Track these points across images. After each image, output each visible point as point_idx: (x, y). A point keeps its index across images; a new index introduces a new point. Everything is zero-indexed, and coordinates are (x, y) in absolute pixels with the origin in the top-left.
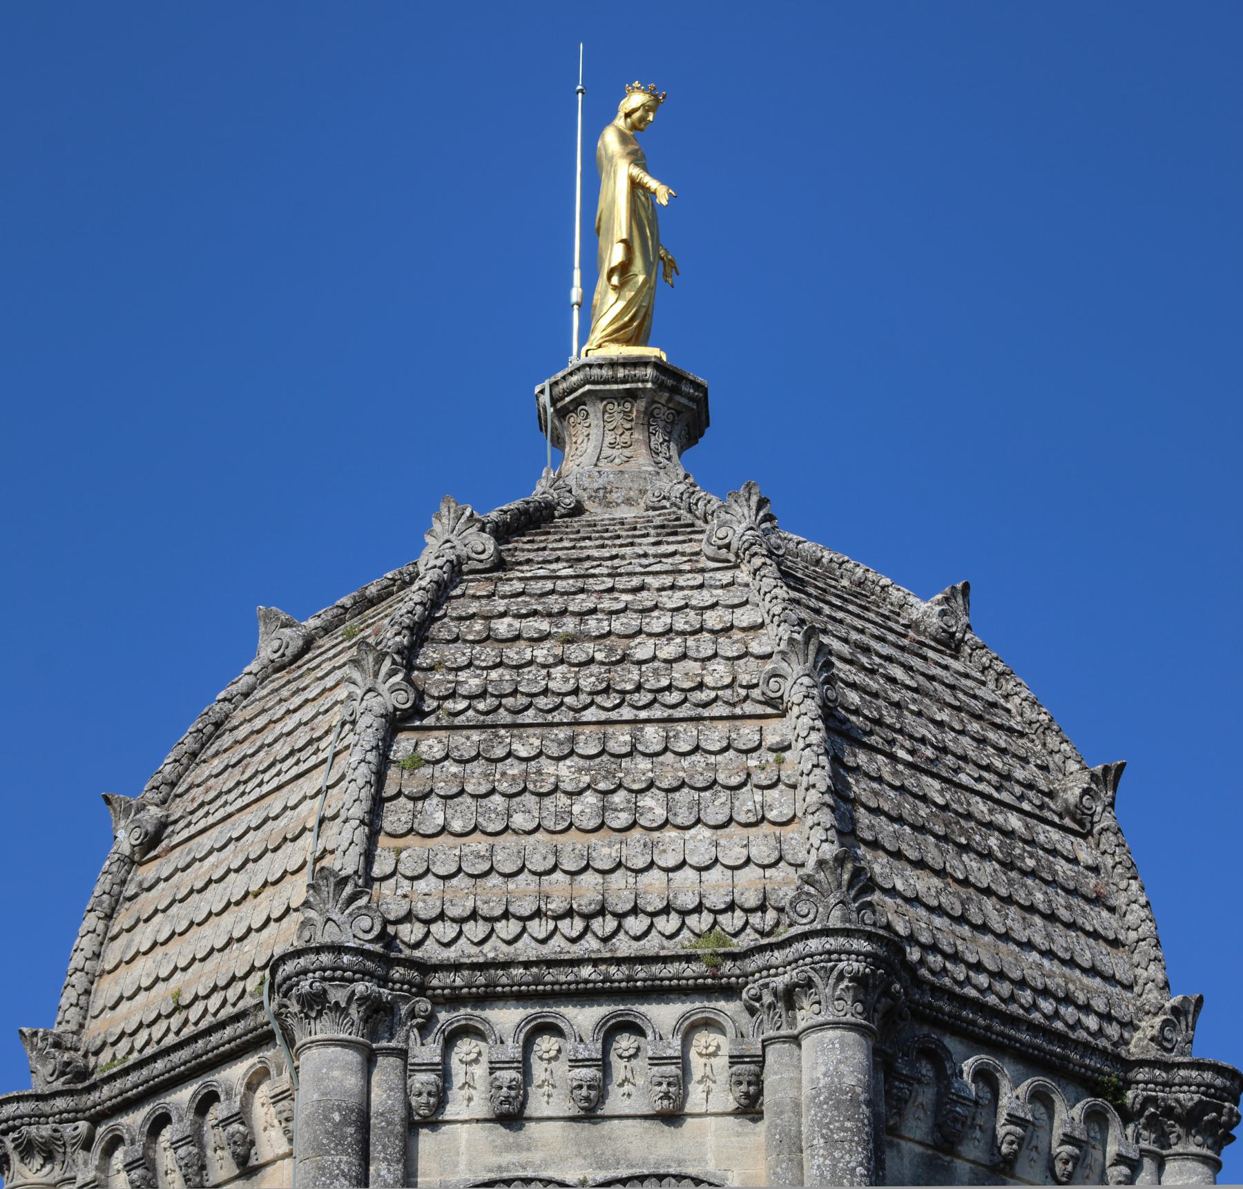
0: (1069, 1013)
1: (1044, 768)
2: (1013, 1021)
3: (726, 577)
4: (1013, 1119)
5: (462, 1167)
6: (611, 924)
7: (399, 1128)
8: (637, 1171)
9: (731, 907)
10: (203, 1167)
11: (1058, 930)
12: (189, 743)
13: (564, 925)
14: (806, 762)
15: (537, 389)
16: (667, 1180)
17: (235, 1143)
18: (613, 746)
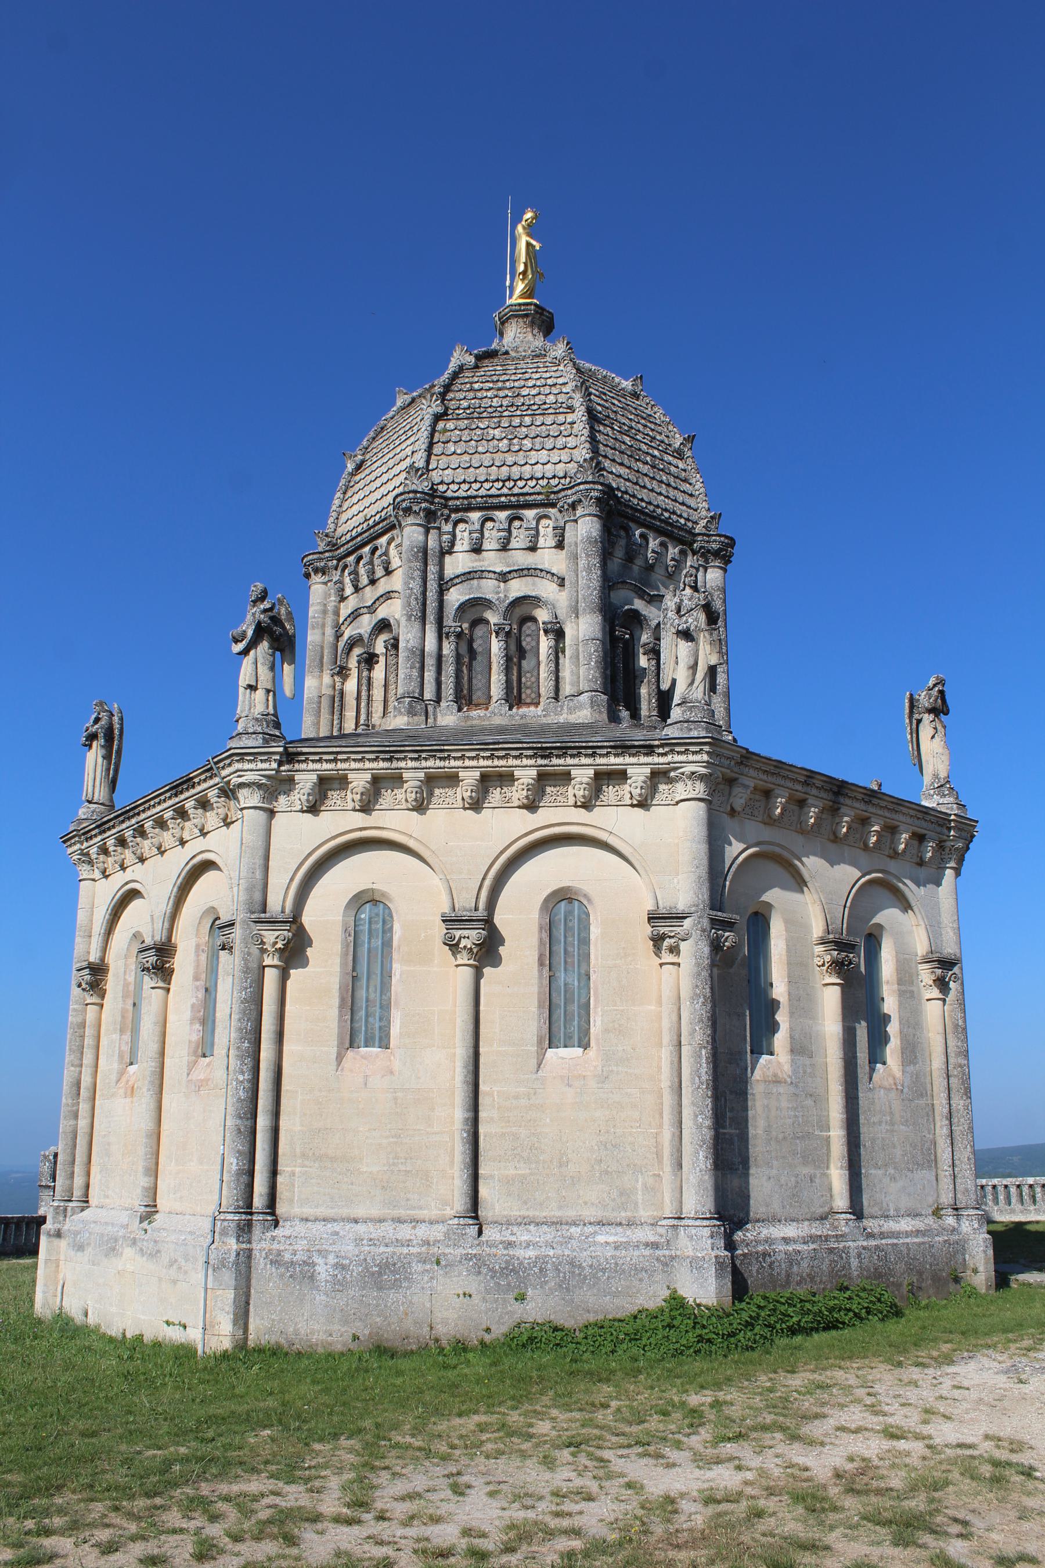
0: (674, 517)
1: (667, 437)
2: (654, 518)
4: (653, 551)
6: (512, 483)
9: (554, 477)
11: (671, 489)
12: (372, 434)
13: (496, 484)
14: (581, 428)
18: (514, 424)
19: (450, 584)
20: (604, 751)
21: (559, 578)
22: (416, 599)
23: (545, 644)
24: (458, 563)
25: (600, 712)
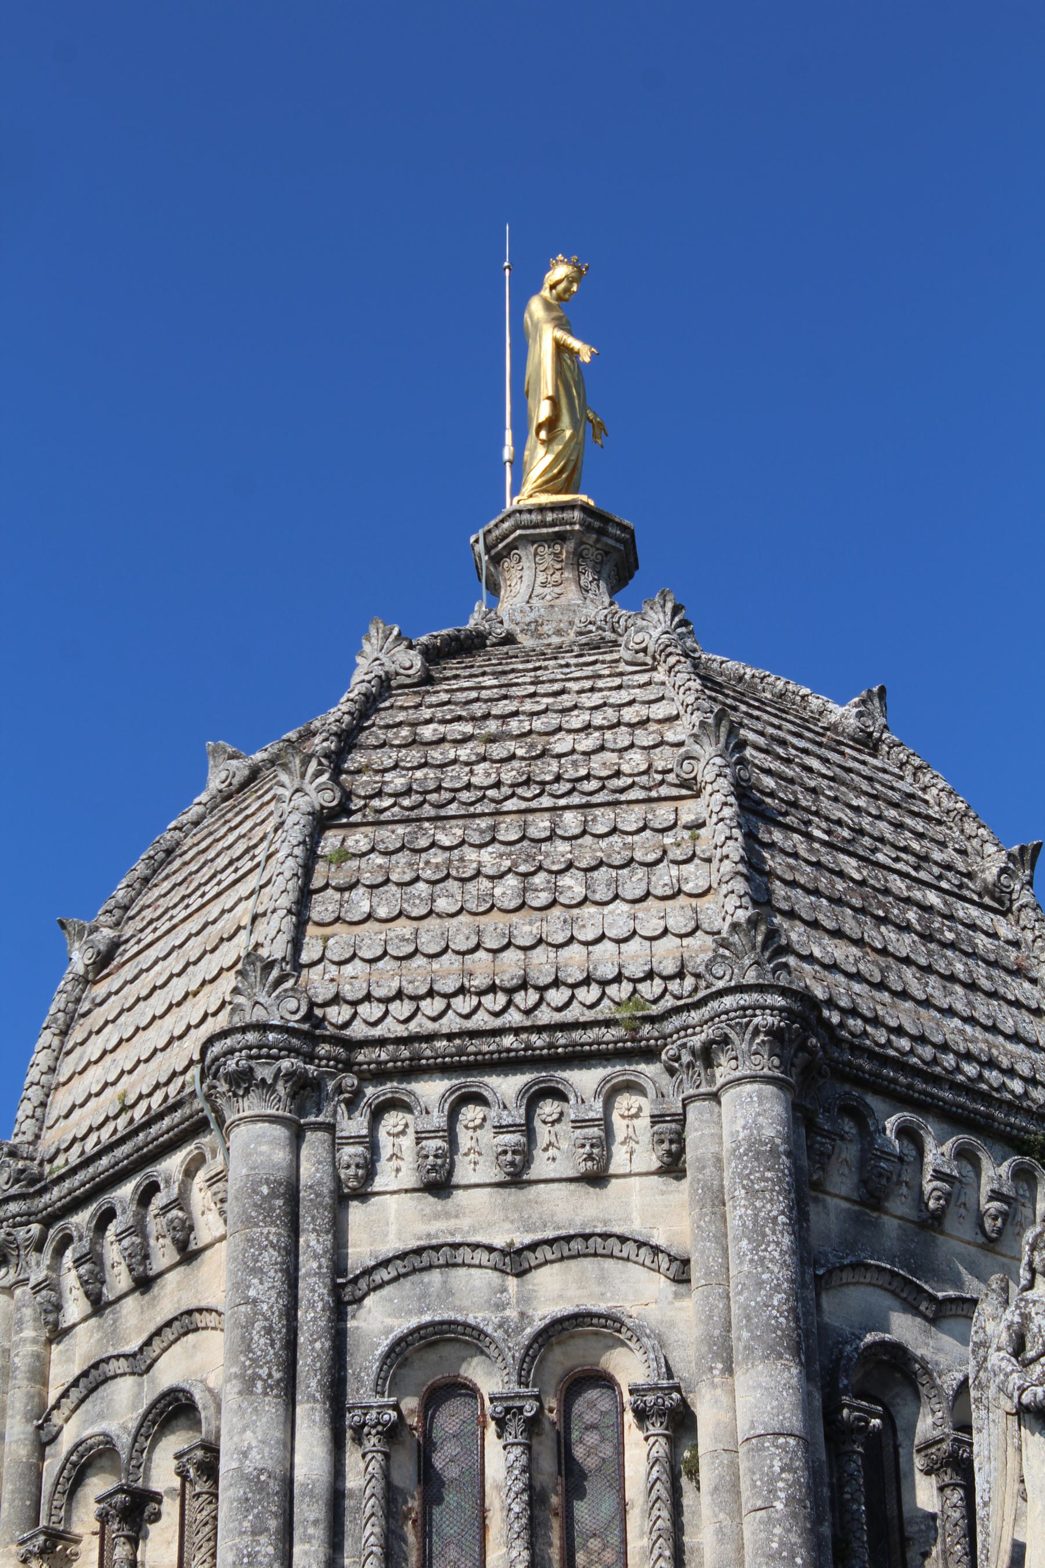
0: (993, 1076)
2: (935, 1080)
3: (644, 678)
4: (938, 1175)
5: (392, 1236)
6: (533, 997)
7: (327, 1200)
8: (563, 1232)
9: (650, 975)
10: (146, 1257)
11: (979, 999)
12: (141, 868)
13: (488, 1000)
14: (721, 837)
15: (472, 539)
16: (593, 1239)
17: (174, 1228)
18: (533, 832)
19: (363, 1284)
21: (672, 1259)
22: (269, 1330)
23: (640, 1451)
24: (387, 1223)
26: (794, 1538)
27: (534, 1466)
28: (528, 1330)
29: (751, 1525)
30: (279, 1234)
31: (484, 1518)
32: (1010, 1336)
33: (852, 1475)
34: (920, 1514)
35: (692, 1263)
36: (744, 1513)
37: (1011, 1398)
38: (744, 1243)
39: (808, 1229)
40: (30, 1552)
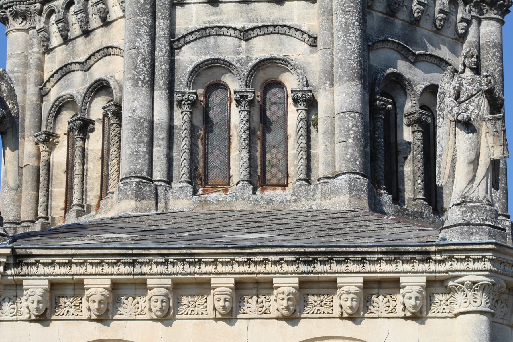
5: (194, 22)
7: (168, 6)
8: (265, 23)
10: (88, 22)
16: (277, 27)
17: (101, 12)
19: (182, 41)
20: (375, 257)
21: (310, 37)
22: (144, 60)
23: (294, 115)
25: (360, 198)
26: (356, 154)
27: (251, 119)
28: (250, 64)
29: (339, 148)
30: (148, 20)
31: (230, 139)
32: (454, 92)
33: (379, 127)
34: (404, 142)
35: (318, 39)
36: (336, 142)
37: (454, 116)
38: (341, 33)
39: (366, 26)
40: (39, 141)
